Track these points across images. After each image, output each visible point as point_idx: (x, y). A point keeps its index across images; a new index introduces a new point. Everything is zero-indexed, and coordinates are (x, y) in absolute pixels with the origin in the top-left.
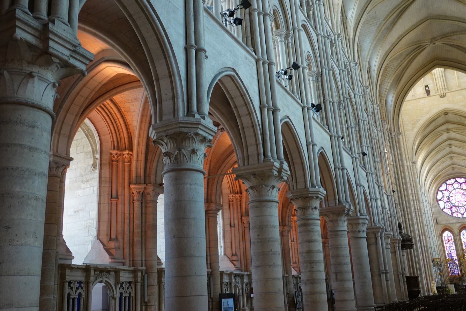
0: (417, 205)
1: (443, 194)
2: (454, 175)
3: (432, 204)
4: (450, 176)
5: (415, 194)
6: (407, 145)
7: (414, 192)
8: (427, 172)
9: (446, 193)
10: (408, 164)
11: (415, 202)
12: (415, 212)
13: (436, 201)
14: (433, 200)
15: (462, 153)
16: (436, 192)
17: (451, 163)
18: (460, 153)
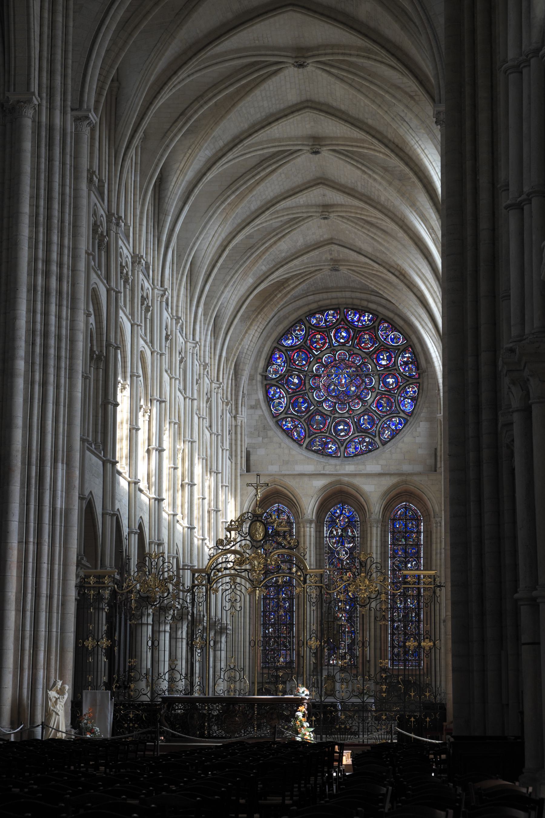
0: (59, 317)
1: (290, 361)
2: (339, 294)
3: (241, 393)
4: (325, 296)
5: (60, 265)
6: (71, 30)
7: (54, 256)
8: (221, 245)
9: (299, 360)
10: (58, 121)
11: (53, 300)
12: (45, 346)
13: (259, 386)
14: (251, 378)
15: (359, 189)
16: (266, 349)
17: (326, 237)
18: (353, 189)
